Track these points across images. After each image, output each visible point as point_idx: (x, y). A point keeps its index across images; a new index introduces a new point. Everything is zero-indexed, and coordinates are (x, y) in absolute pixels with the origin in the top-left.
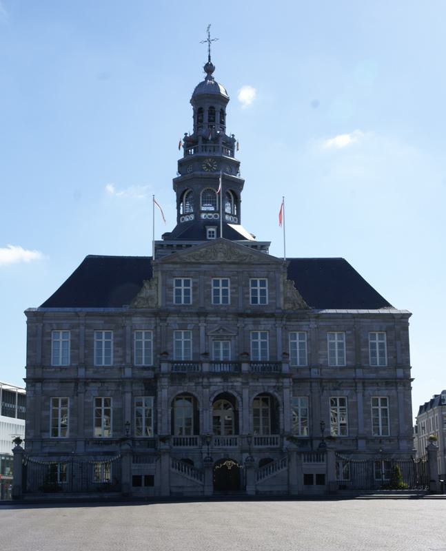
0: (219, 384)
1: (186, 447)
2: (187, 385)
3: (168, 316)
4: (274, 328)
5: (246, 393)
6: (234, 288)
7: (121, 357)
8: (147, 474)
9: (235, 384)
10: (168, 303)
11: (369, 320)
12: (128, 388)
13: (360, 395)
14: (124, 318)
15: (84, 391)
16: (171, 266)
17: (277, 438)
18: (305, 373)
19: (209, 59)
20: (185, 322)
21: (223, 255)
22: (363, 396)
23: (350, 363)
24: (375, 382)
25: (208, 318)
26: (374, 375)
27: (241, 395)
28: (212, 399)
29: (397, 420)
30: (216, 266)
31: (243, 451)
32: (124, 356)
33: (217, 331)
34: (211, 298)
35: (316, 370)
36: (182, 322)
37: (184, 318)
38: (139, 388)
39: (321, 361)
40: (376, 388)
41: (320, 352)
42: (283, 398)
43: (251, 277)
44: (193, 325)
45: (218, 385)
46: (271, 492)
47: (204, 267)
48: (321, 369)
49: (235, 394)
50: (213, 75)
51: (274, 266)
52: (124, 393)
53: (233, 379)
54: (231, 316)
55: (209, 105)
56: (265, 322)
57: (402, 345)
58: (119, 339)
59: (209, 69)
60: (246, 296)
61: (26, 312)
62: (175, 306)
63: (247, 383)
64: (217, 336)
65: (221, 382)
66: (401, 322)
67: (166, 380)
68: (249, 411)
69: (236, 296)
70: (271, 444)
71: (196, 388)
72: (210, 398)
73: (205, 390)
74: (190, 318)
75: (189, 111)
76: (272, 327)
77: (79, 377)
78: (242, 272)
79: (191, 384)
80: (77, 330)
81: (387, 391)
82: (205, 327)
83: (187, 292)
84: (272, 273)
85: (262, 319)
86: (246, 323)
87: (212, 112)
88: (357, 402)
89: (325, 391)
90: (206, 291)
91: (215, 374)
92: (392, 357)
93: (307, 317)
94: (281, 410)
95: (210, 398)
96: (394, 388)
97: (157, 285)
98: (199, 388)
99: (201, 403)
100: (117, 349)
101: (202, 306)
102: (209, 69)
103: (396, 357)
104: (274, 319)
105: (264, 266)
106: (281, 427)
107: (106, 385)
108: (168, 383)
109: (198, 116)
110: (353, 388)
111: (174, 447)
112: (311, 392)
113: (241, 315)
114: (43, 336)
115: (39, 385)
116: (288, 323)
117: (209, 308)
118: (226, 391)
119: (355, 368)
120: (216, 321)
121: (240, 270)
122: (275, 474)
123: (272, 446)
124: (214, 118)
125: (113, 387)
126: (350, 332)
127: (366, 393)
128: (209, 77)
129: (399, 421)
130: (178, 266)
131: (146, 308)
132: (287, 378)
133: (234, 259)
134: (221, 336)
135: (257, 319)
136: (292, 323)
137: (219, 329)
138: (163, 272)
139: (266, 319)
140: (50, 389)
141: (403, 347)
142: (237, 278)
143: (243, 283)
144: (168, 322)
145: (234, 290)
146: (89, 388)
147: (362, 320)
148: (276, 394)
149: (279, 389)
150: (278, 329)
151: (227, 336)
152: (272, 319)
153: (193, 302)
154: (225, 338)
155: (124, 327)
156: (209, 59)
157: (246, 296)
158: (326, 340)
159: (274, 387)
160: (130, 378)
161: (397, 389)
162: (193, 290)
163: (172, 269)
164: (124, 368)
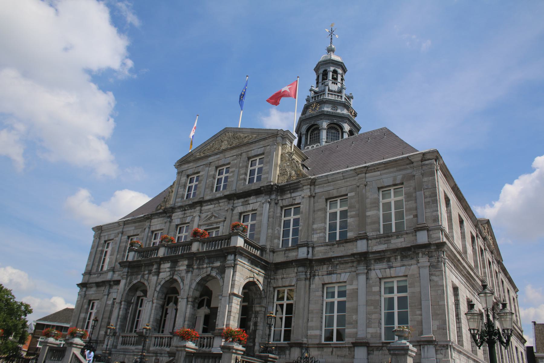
0: (168, 270)
11: (379, 173)
13: (362, 278)
15: (107, 293)
16: (186, 166)
18: (292, 255)
22: (367, 279)
24: (381, 257)
25: (203, 208)
26: (386, 245)
27: (183, 280)
28: (158, 289)
29: (418, 312)
33: (209, 219)
34: (213, 187)
35: (305, 249)
36: (182, 216)
39: (315, 238)
40: (384, 265)
41: (315, 226)
47: (211, 159)
48: (313, 248)
49: (179, 280)
51: (271, 140)
54: (223, 200)
56: (255, 201)
57: (426, 198)
61: (93, 229)
64: (209, 225)
66: (424, 165)
68: (188, 301)
74: (190, 211)
76: (260, 206)
78: (241, 154)
80: (117, 239)
81: (403, 268)
82: (200, 216)
84: (268, 147)
85: (252, 198)
87: (325, 74)
88: (357, 289)
89: (317, 278)
92: (412, 216)
93: (301, 186)
96: (414, 262)
103: (416, 216)
104: (263, 195)
105: (261, 143)
110: (353, 269)
114: (97, 247)
115: (84, 289)
116: (279, 198)
121: (240, 152)
124: (327, 77)
126: (353, 194)
127: (373, 274)
129: (421, 315)
130: (191, 164)
132: (231, 253)
134: (211, 224)
135: (246, 199)
139: (254, 197)
140: (91, 293)
141: (428, 200)
142: (236, 161)
143: (241, 165)
144: (173, 218)
146: (112, 291)
147: (367, 175)
148: (219, 277)
151: (217, 223)
152: (261, 195)
154: (215, 226)
158: (325, 210)
161: (418, 262)
163: (187, 168)
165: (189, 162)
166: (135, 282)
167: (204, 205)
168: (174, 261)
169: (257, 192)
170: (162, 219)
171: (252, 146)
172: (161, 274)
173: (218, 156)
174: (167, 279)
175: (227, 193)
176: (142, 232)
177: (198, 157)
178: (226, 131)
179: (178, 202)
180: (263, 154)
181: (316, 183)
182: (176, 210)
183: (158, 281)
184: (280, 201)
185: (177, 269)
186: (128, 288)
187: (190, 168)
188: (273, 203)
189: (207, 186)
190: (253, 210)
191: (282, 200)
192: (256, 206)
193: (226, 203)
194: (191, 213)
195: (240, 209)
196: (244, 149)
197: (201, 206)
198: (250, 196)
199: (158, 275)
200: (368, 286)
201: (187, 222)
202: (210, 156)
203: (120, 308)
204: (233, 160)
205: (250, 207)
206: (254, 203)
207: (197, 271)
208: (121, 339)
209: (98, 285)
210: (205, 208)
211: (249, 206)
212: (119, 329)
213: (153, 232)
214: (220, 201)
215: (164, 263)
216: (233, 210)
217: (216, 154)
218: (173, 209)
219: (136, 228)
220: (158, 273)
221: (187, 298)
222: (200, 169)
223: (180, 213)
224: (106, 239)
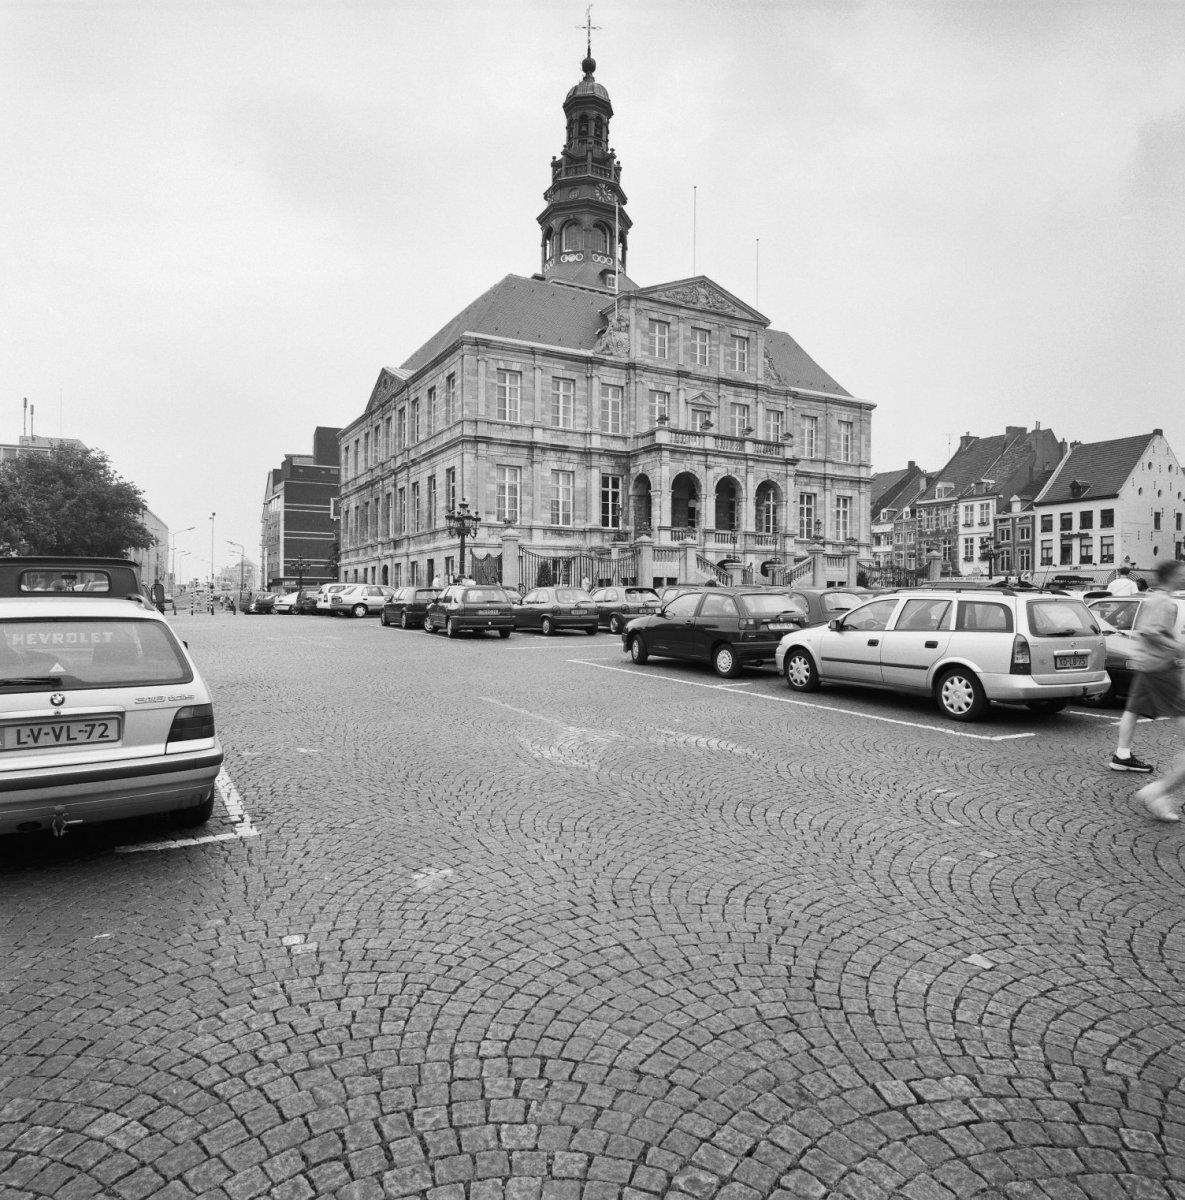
5: (751, 478)
8: (670, 576)
16: (647, 303)
19: (589, 53)
23: (821, 456)
30: (698, 314)
32: (589, 419)
38: (607, 466)
40: (841, 485)
45: (722, 468)
50: (594, 74)
55: (588, 113)
59: (589, 66)
75: (562, 120)
77: (535, 440)
80: (531, 374)
83: (662, 341)
97: (628, 326)
99: (703, 488)
100: (578, 407)
102: (589, 66)
103: (860, 453)
107: (567, 455)
109: (580, 127)
113: (721, 381)
115: (482, 447)
117: (689, 368)
119: (825, 462)
125: (575, 457)
128: (588, 78)
138: (638, 311)
145: (714, 349)
151: (708, 406)
155: (591, 377)
156: (589, 53)
162: (669, 341)
164: (590, 434)
171: (737, 322)
175: (713, 374)
178: (703, 281)
180: (748, 339)
192: (749, 401)
195: (732, 399)
200: (832, 501)
205: (742, 401)
209: (515, 444)
219: (567, 368)
224: (502, 367)
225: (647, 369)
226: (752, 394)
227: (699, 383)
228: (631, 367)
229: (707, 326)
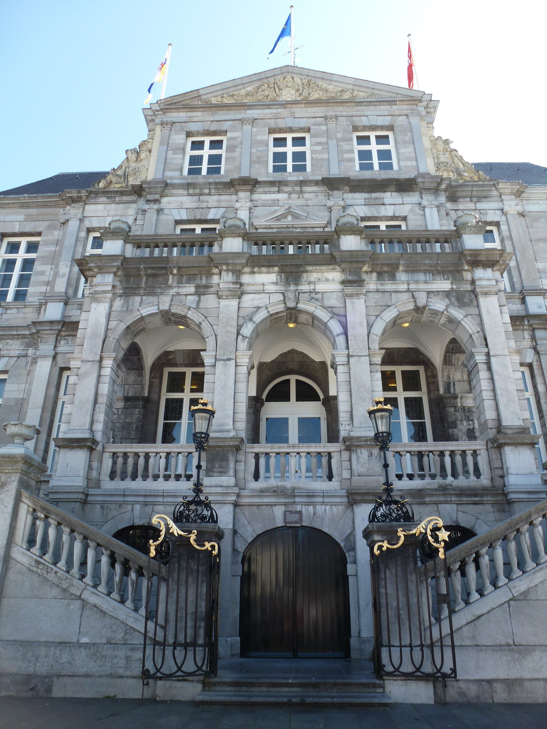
0: (273, 288)
1: (150, 485)
2: (173, 291)
3: (162, 196)
4: (422, 212)
5: (357, 310)
6: (318, 144)
7: (48, 283)
9: (320, 287)
10: (168, 174)
12: (47, 348)
14: (68, 207)
17: (475, 453)
20: (204, 205)
21: (294, 92)
25: (256, 197)
28: (248, 330)
31: (354, 498)
33: (278, 218)
35: (539, 299)
36: (195, 205)
37: (202, 198)
42: (481, 324)
43: (355, 129)
44: (222, 210)
46: (510, 684)
51: (405, 108)
52: (34, 361)
53: (314, 276)
54: (315, 188)
56: (399, 201)
58: (53, 248)
60: (346, 156)
62: (184, 178)
63: (360, 282)
65: (276, 284)
67: (109, 278)
69: (325, 156)
70: (455, 475)
71: (198, 302)
72: (239, 328)
73: (223, 302)
74: (216, 198)
76: (412, 210)
78: (336, 117)
79: (183, 291)
84: (400, 118)
85: (388, 194)
86: (350, 202)
90: (254, 150)
91: (257, 263)
94: (480, 358)
95: (239, 328)
97: (150, 151)
98: (209, 301)
101: (245, 173)
104: (417, 194)
106: (490, 414)
108: (114, 287)
111: (108, 485)
112: (537, 352)
113: (331, 184)
116: (449, 205)
118: (291, 304)
120: (278, 200)
121: (333, 114)
122: (521, 585)
123: (462, 482)
130: (199, 114)
131: (121, 187)
133: (315, 96)
135: (374, 195)
136: (461, 206)
137: (284, 216)
139: (394, 194)
142: (324, 128)
143: (339, 136)
148: (457, 313)
149: (468, 298)
150: (427, 210)
152: (411, 193)
153: (225, 171)
157: (346, 156)
159: (447, 294)
160: (52, 322)
163: (185, 119)
164: (46, 303)
165: (193, 108)
166: (146, 311)
167: (260, 190)
168: (292, 272)
169: (404, 186)
170: (122, 206)
172: (245, 298)
173: (274, 111)
174: (273, 310)
176: (48, 228)
177: (213, 102)
179: (172, 178)
181: (524, 195)
182: (174, 191)
183: (243, 313)
184: (452, 213)
185: (304, 287)
186: (123, 326)
187: (195, 119)
188: (443, 213)
189: (255, 159)
190: (394, 218)
191: (456, 210)
193: (321, 197)
194: (219, 201)
196: (340, 110)
197: (252, 191)
198: (384, 192)
199: (240, 298)
201: (210, 217)
202: (250, 107)
203: (99, 376)
204: (315, 124)
205: (389, 211)
206: (393, 204)
207: (377, 296)
208: (108, 463)
210: (261, 196)
211: (383, 207)
212: (104, 433)
213: (89, 230)
214: (305, 189)
215: (253, 273)
216: (344, 208)
217: (268, 106)
218: (165, 187)
219: (29, 219)
220: (239, 292)
221: (369, 355)
222: (225, 126)
223: (185, 198)
225: (165, 187)
226: (412, 198)
227: (282, 196)
228: (138, 191)
229: (303, 123)
